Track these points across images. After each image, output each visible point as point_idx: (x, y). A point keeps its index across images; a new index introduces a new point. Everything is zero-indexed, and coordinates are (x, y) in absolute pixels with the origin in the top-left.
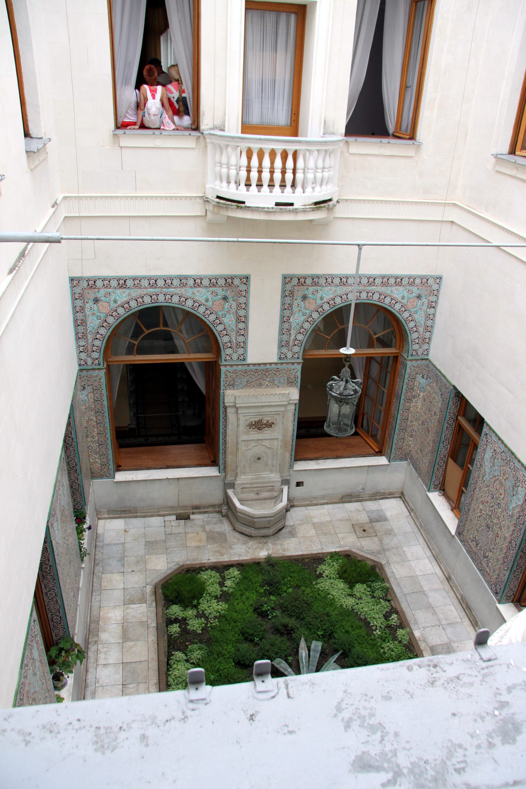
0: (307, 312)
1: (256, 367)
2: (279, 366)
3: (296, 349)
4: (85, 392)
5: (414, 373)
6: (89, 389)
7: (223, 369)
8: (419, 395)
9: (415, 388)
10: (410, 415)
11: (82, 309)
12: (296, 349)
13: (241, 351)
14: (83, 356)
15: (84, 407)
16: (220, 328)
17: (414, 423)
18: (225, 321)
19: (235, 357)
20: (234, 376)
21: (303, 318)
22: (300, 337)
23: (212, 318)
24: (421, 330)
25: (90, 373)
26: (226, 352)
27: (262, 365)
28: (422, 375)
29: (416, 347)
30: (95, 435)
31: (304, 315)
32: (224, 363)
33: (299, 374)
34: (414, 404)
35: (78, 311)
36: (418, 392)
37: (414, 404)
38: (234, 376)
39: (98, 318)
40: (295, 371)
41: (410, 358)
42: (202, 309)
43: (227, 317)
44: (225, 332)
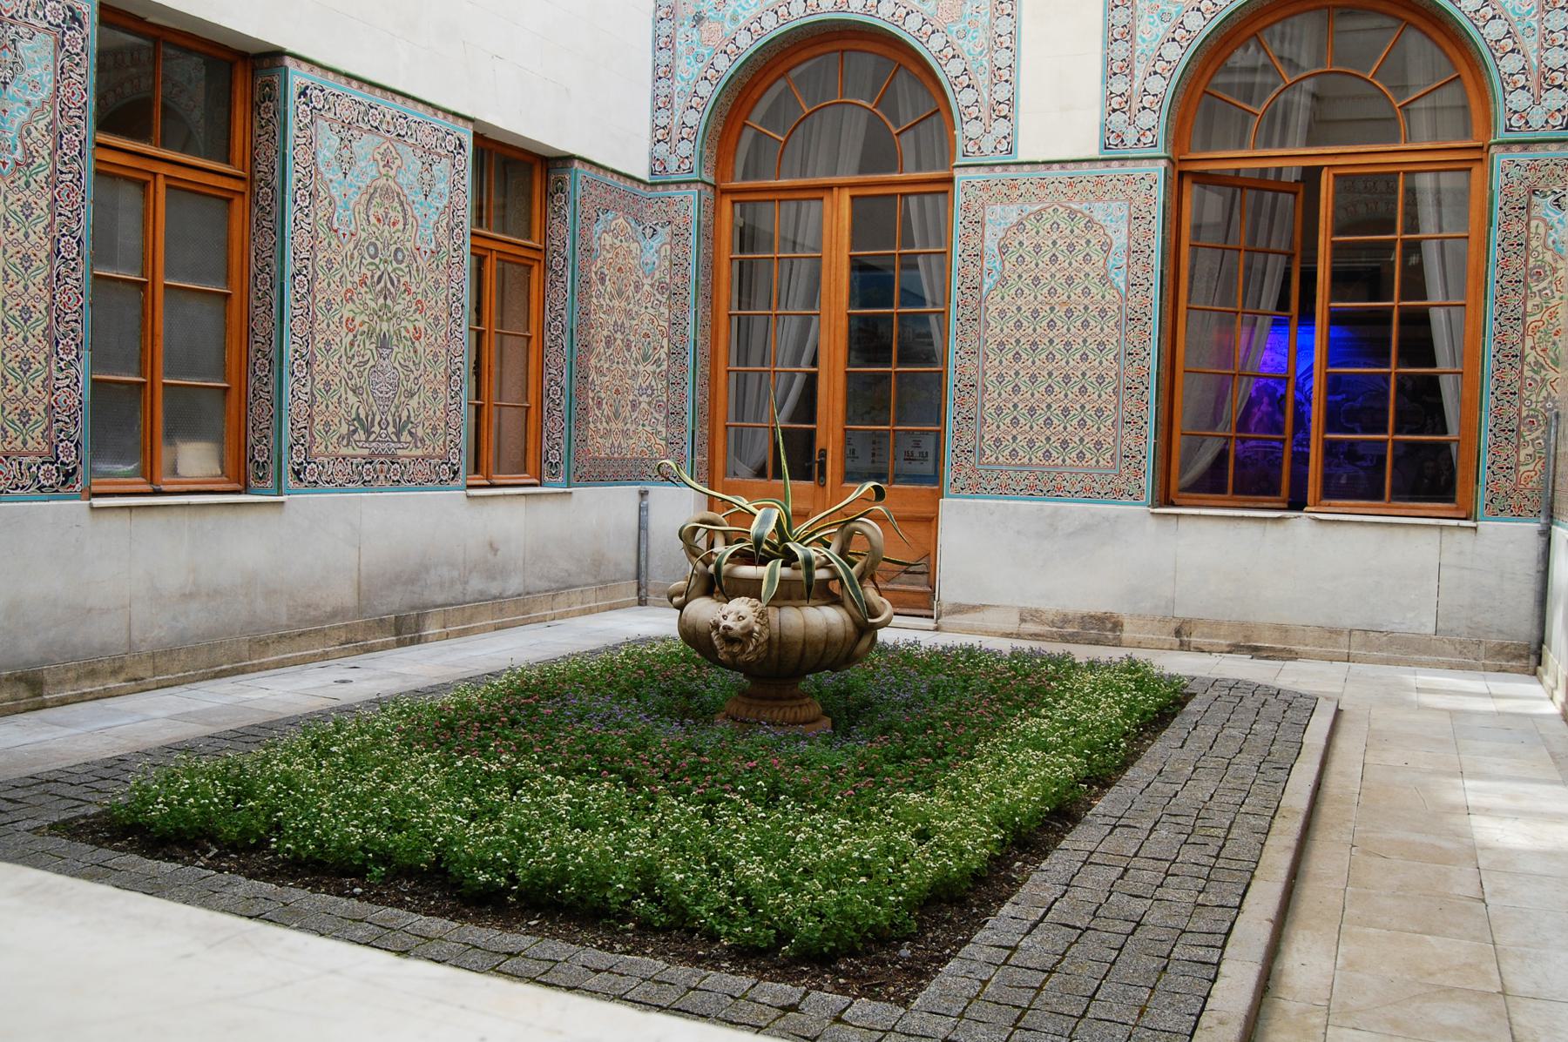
0: (1173, 10)
1: (1042, 171)
2: (1100, 168)
3: (1147, 119)
4: (655, 243)
5: (1522, 190)
6: (664, 233)
7: (957, 174)
8: (1555, 270)
9: (1534, 243)
10: (1529, 342)
11: (671, 39)
12: (1147, 119)
13: (1001, 127)
14: (662, 148)
15: (647, 281)
16: (954, 68)
17: (1551, 375)
18: (965, 48)
19: (987, 145)
20: (986, 197)
21: (1162, 29)
22: (1157, 85)
23: (936, 43)
24: (1531, 45)
25: (672, 190)
26: (967, 131)
27: (1056, 166)
28: (1552, 197)
29: (1519, 100)
30: (663, 356)
31: (1166, 18)
32: (960, 160)
33: (1159, 192)
34: (1537, 300)
35: (663, 44)
36: (1548, 257)
37: (1537, 300)
38: (986, 197)
39: (699, 58)
40: (1146, 184)
41: (1503, 136)
42: (913, 23)
43: (969, 37)
44: (965, 80)
